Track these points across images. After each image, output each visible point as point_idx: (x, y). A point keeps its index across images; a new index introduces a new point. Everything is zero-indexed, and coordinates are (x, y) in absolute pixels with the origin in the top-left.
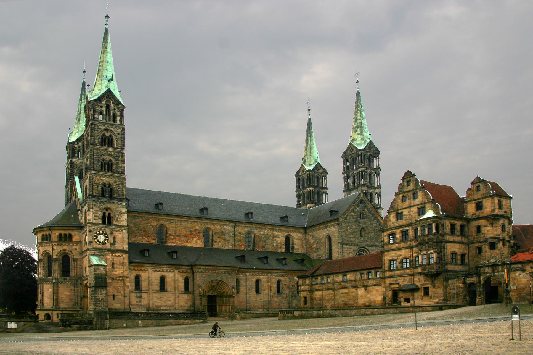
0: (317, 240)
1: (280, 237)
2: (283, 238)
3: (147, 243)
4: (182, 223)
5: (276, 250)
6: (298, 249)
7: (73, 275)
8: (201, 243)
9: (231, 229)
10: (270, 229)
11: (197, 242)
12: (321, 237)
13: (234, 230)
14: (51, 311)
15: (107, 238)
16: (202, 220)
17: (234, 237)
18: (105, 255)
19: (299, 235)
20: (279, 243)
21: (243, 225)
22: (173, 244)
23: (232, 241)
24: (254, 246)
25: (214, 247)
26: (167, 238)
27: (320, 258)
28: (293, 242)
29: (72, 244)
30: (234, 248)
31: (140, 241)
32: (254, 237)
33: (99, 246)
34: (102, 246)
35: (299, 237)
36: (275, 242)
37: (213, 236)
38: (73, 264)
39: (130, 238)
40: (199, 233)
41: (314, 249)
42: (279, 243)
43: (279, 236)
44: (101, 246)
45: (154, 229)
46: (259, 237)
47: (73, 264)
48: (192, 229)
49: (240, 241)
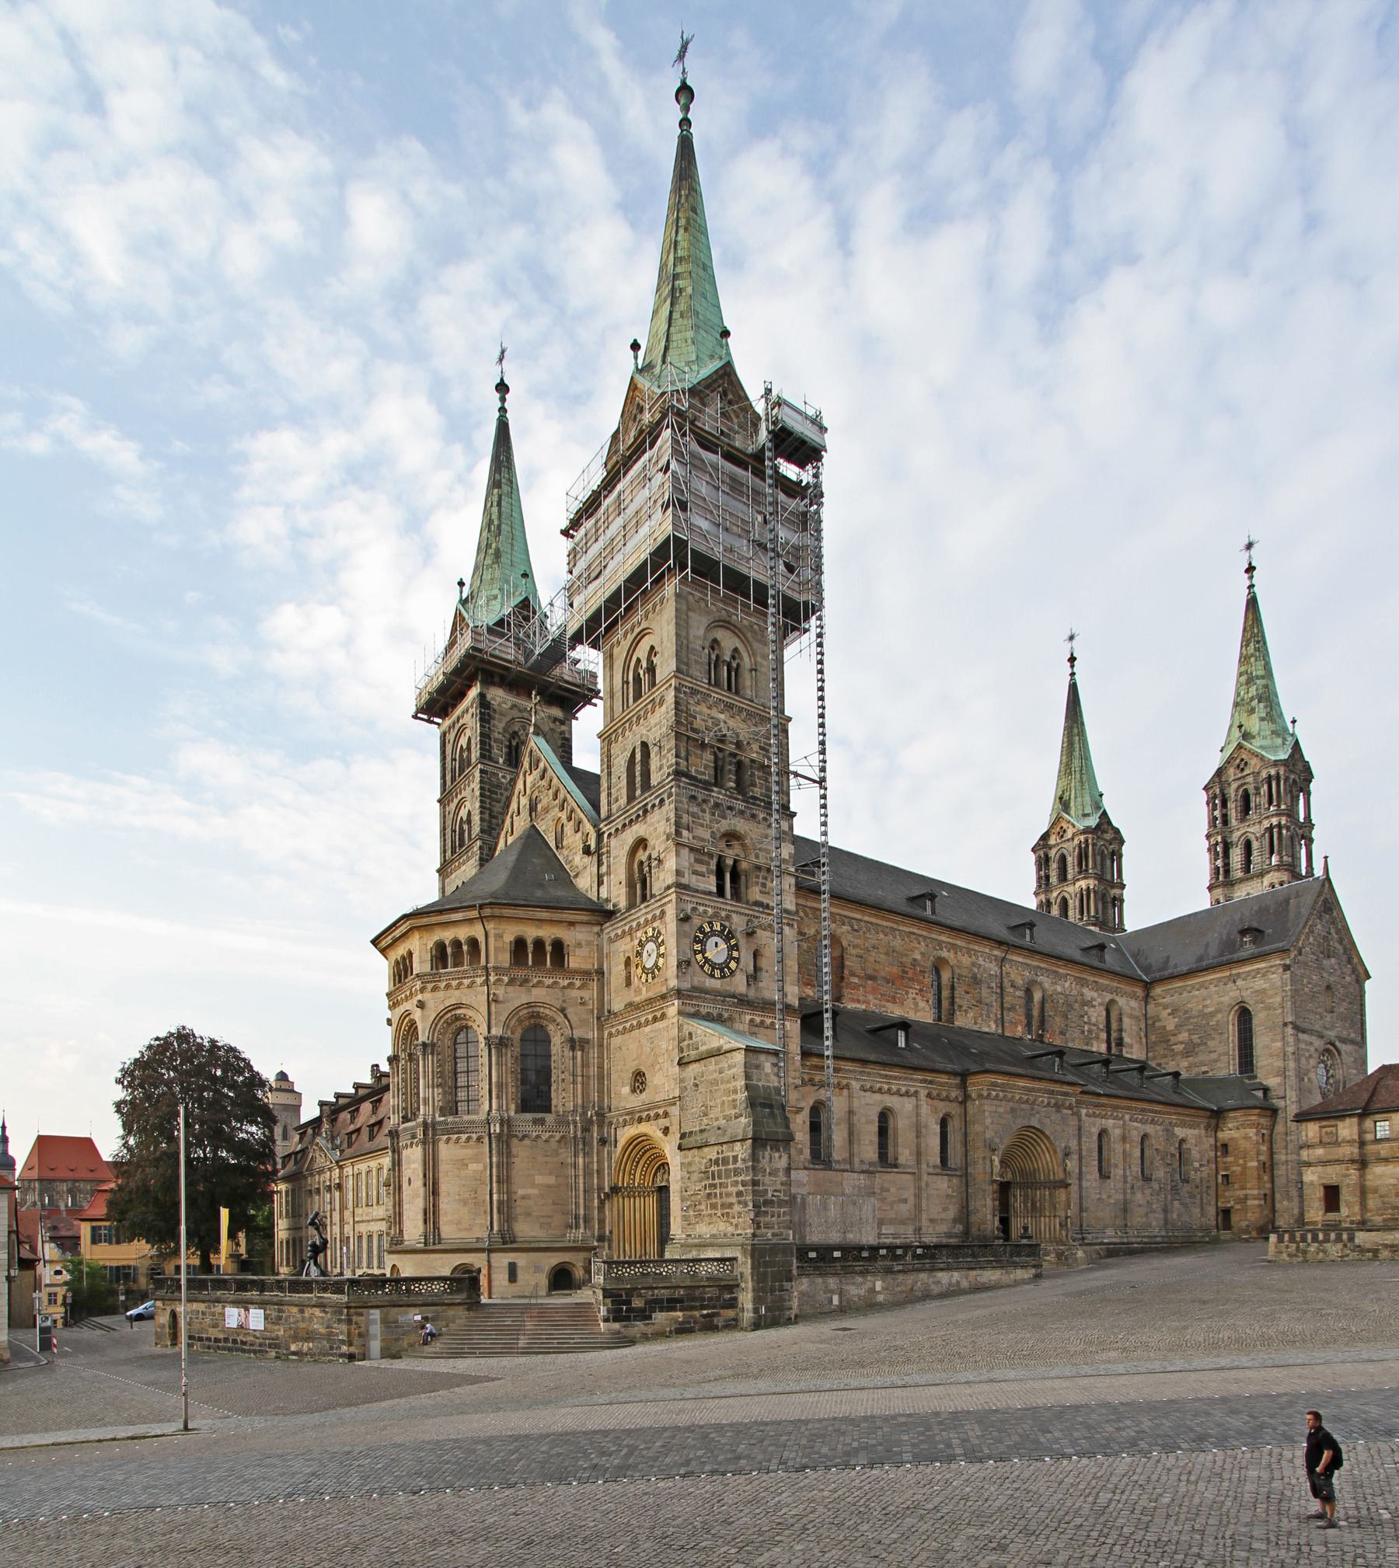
0: (1195, 1020)
2: (1102, 1008)
4: (881, 936)
8: (928, 1008)
9: (994, 969)
10: (1076, 978)
11: (916, 1004)
12: (1210, 1010)
15: (735, 954)
16: (930, 930)
20: (1094, 1025)
21: (1020, 960)
22: (859, 1006)
23: (996, 1008)
27: (1207, 1072)
33: (710, 983)
36: (1086, 1019)
41: (1181, 1047)
42: (1094, 1025)
44: (715, 984)
45: (809, 947)
48: (904, 960)
49: (1012, 1009)
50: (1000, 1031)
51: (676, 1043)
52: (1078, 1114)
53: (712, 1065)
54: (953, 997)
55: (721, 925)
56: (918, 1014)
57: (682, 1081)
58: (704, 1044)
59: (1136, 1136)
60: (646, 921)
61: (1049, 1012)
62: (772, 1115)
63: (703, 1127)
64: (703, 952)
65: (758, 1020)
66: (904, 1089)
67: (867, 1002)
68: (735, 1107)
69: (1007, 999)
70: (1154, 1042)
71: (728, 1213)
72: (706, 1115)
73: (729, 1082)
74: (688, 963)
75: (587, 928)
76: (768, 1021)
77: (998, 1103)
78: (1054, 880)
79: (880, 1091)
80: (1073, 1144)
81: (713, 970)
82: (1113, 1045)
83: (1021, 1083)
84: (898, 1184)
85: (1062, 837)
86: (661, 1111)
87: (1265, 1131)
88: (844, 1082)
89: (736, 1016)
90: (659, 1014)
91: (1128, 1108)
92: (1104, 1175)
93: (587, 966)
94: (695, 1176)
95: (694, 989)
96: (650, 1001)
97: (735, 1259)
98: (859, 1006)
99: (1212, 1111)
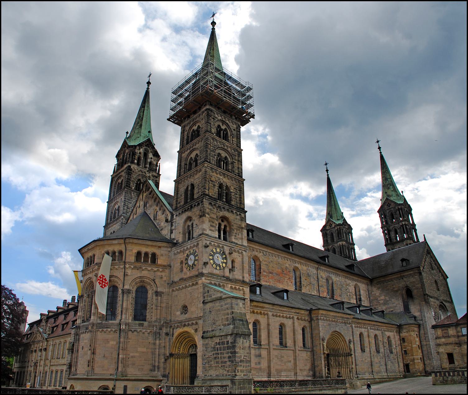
2: (353, 287)
5: (349, 300)
6: (364, 301)
7: (154, 319)
9: (315, 271)
11: (288, 284)
14: (113, 382)
17: (318, 281)
22: (267, 283)
23: (316, 286)
24: (333, 295)
25: (303, 291)
28: (360, 293)
29: (156, 269)
30: (318, 295)
34: (219, 271)
38: (154, 301)
43: (350, 285)
47: (154, 301)
50: (318, 295)
51: (202, 294)
52: (352, 326)
53: (217, 304)
54: (301, 281)
55: (220, 250)
56: (289, 287)
57: (204, 310)
58: (215, 295)
59: (372, 335)
60: (191, 247)
61: (335, 288)
62: (243, 324)
63: (213, 329)
64: (213, 259)
65: (234, 286)
66: (288, 316)
67: (270, 282)
68: (228, 321)
69: (320, 282)
70: (372, 300)
71: (224, 366)
72: (214, 324)
73: (225, 310)
74: (207, 263)
75: (166, 249)
77: (324, 322)
78: (329, 241)
79: (279, 316)
80: (351, 338)
81: (216, 267)
82: (358, 300)
83: (332, 314)
84: (288, 354)
85: (331, 227)
86: (194, 322)
87: (417, 333)
88: (266, 312)
89: (225, 285)
90: (194, 283)
91: (369, 324)
92: (363, 350)
93: (165, 264)
94: (209, 349)
96: (191, 278)
97: (228, 386)
98: (267, 283)
99: (398, 325)
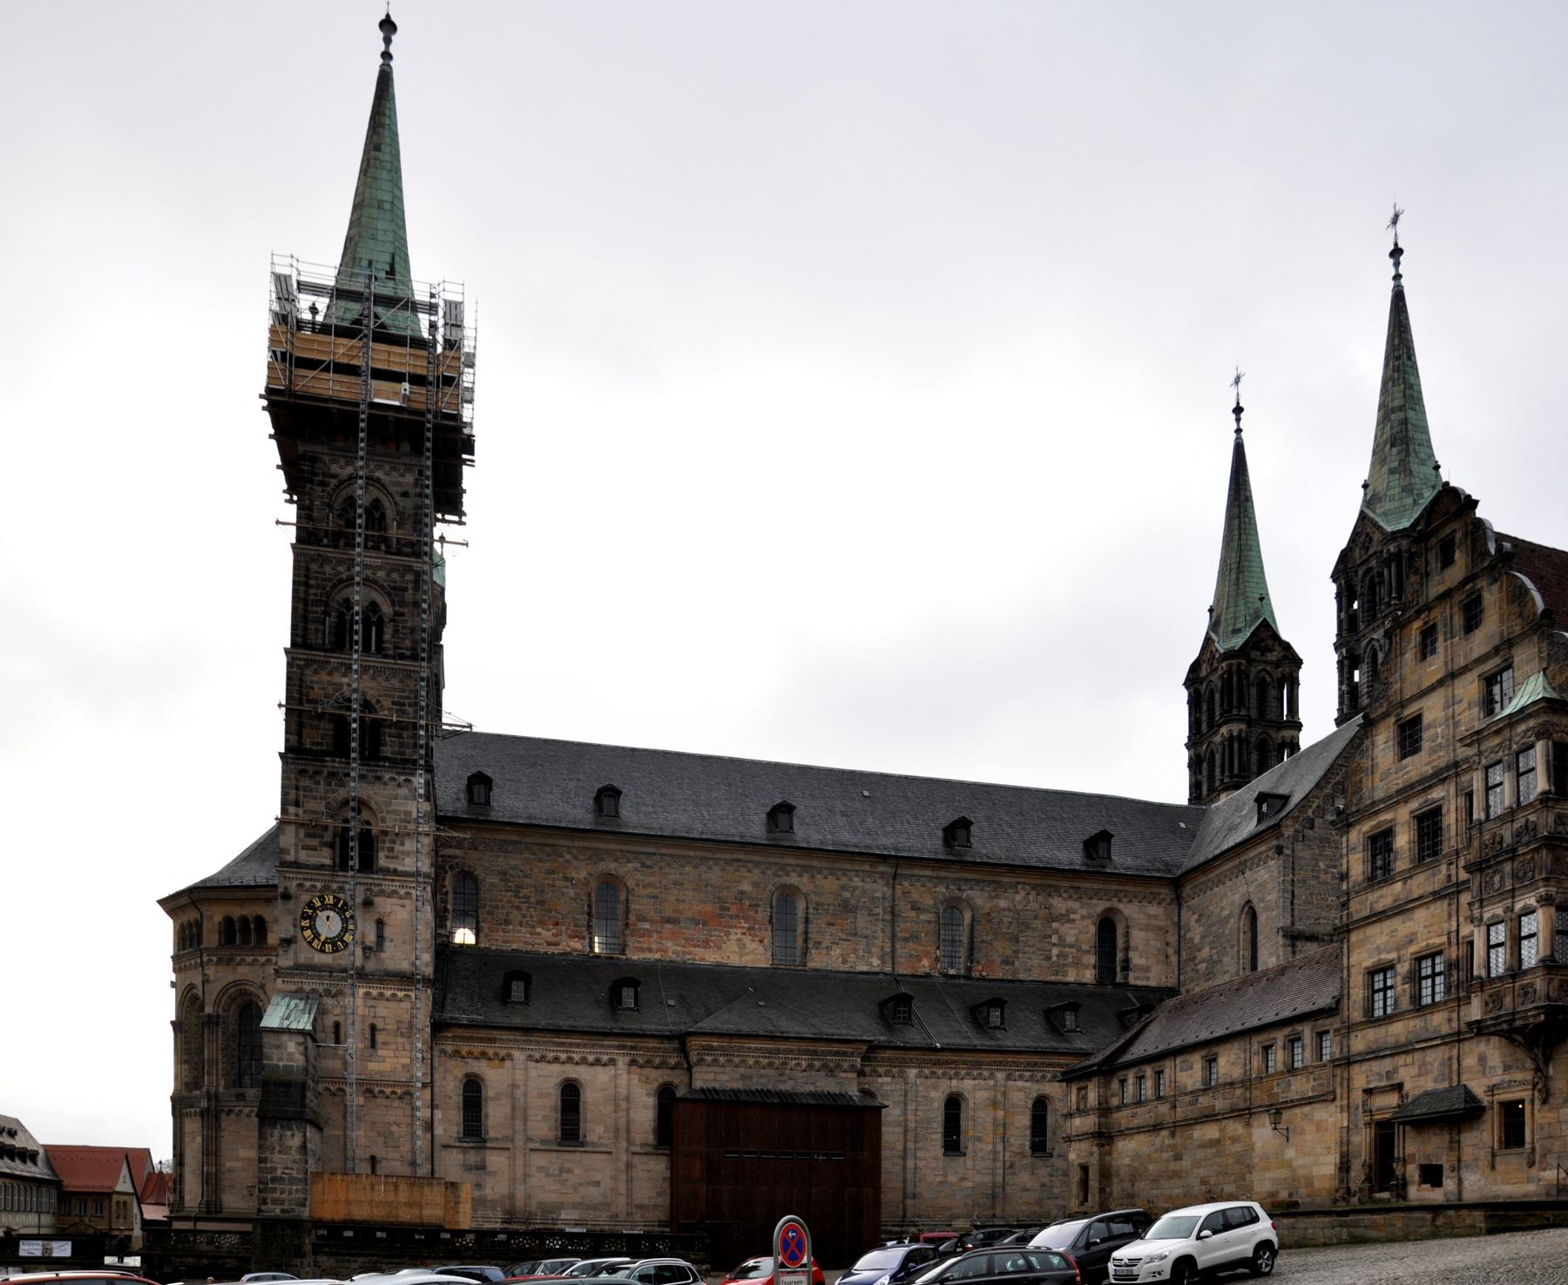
1: (1074, 920)
2: (1089, 922)
3: (551, 950)
8: (761, 949)
9: (880, 889)
10: (1034, 887)
11: (742, 947)
13: (894, 894)
17: (893, 922)
18: (340, 993)
19: (1154, 909)
21: (928, 873)
23: (881, 939)
26: (628, 932)
31: (525, 943)
32: (973, 920)
35: (1150, 917)
36: (1055, 939)
37: (807, 921)
39: (486, 931)
40: (754, 906)
43: (1072, 916)
45: (576, 894)
46: (990, 921)
48: (724, 893)
49: (913, 937)
54: (806, 933)
61: (982, 935)
76: (388, 993)
88: (502, 1053)
89: (348, 991)
95: (297, 967)
